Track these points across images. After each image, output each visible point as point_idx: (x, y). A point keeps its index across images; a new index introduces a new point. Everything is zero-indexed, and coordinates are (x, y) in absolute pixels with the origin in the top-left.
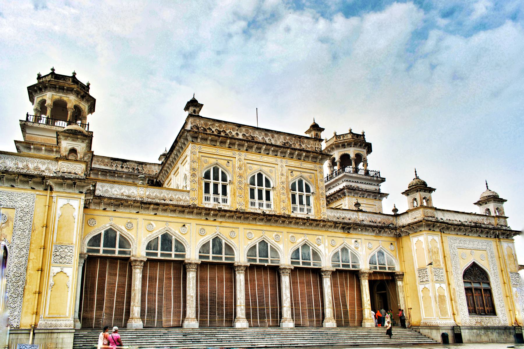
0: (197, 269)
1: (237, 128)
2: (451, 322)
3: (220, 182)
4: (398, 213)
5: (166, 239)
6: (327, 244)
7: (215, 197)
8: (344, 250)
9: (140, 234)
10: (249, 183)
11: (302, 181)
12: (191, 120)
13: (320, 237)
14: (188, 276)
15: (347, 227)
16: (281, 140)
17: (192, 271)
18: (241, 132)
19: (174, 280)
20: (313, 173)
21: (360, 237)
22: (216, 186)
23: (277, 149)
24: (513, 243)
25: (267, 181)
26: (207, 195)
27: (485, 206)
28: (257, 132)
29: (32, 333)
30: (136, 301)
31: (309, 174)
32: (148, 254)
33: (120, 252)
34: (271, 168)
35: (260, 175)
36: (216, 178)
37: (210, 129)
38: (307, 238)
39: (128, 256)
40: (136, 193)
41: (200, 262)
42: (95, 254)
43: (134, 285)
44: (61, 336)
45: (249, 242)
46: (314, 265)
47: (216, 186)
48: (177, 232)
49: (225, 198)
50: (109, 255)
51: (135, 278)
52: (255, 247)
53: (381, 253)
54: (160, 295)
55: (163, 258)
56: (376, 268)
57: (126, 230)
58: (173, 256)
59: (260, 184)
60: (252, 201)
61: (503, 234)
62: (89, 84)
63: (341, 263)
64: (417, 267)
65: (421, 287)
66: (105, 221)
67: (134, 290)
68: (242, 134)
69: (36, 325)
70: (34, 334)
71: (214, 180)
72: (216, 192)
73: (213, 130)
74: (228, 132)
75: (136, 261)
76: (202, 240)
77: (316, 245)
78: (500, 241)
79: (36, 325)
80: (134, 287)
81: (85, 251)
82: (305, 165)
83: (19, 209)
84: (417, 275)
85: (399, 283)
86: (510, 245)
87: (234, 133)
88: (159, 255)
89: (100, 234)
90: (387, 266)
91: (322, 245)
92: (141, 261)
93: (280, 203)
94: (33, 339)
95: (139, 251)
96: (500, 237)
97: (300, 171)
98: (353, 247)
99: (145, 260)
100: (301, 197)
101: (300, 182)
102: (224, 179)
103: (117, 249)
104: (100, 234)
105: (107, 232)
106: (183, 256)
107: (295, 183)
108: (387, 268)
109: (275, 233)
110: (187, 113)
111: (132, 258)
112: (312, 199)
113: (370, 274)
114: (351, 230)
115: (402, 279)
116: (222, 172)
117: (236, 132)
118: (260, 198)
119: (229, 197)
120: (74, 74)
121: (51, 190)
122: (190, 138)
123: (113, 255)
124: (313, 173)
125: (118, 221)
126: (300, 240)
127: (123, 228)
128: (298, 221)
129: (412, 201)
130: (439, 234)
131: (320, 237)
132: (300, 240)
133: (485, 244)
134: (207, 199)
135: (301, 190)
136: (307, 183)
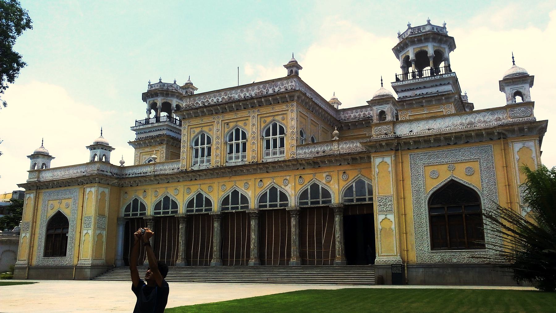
8: (315, 187)
13: (288, 178)
15: (316, 163)
25: (244, 134)
31: (281, 116)
46: (280, 207)
63: (309, 201)
73: (200, 103)
76: (188, 197)
77: (283, 186)
81: (123, 215)
91: (289, 185)
92: (150, 219)
93: (254, 152)
97: (272, 116)
100: (275, 141)
108: (367, 199)
116: (208, 137)
119: (211, 157)
126: (268, 183)
131: (288, 178)
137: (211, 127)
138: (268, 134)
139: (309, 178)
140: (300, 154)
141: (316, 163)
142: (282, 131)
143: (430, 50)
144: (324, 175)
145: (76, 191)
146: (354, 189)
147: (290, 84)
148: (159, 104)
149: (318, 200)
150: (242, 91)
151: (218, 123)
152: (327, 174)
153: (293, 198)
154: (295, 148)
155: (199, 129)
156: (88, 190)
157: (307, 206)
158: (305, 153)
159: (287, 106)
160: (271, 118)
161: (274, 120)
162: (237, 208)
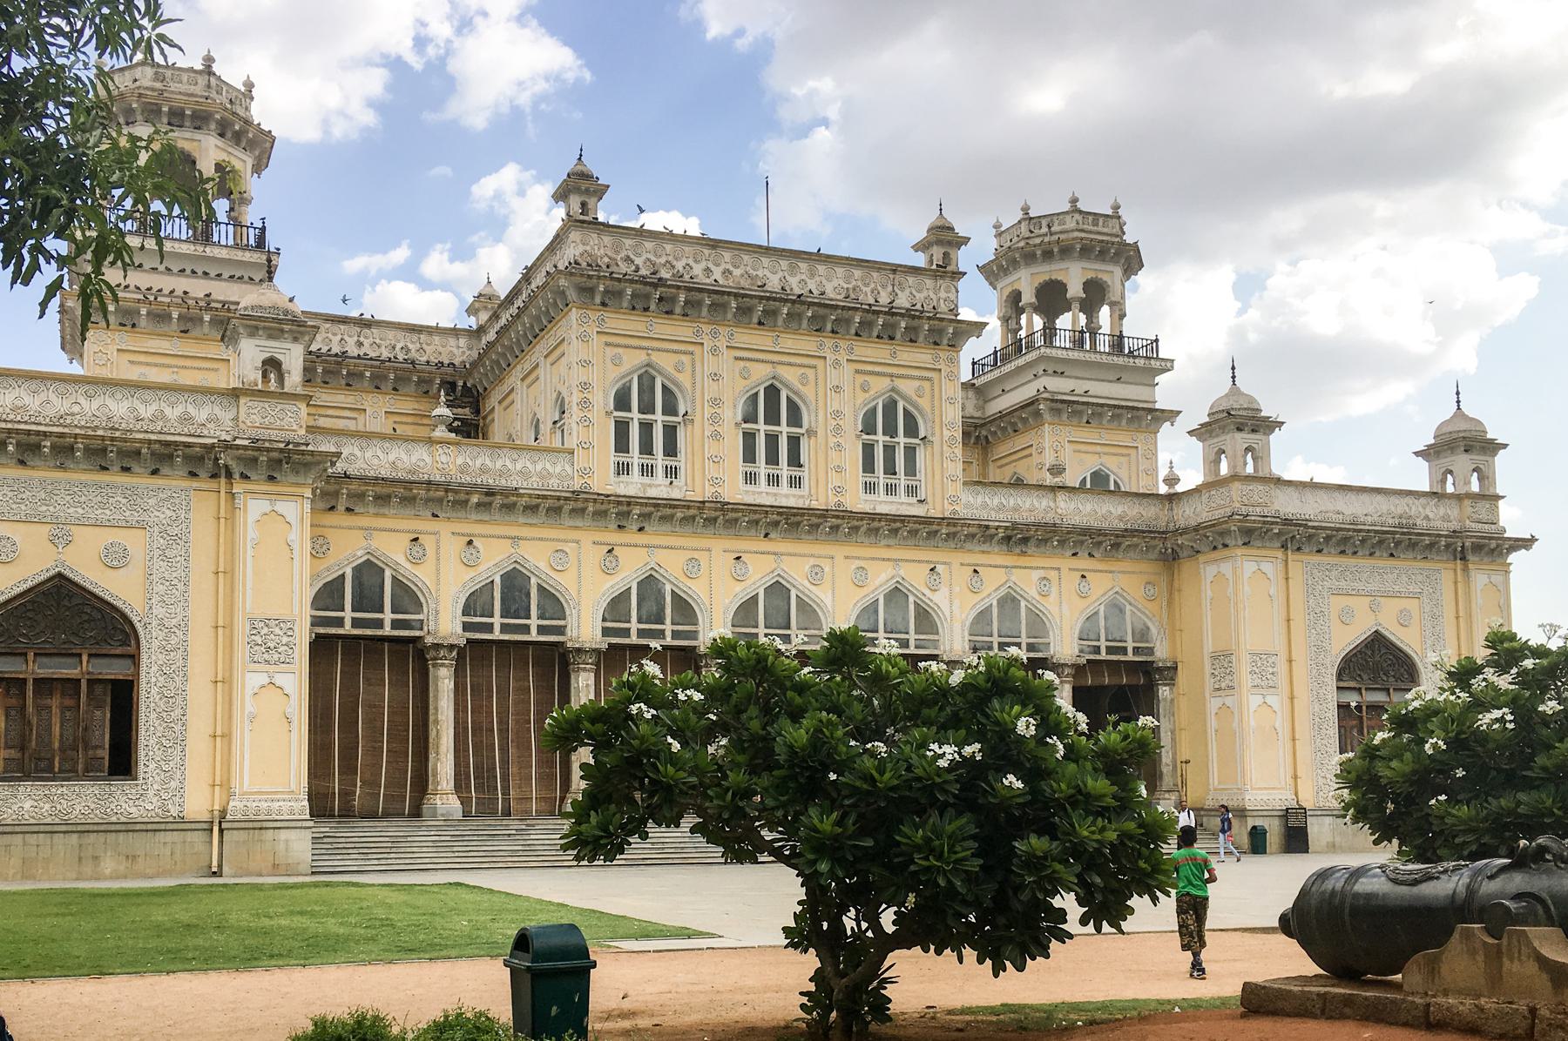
0: (598, 664)
1: (707, 252)
2: (1281, 798)
3: (659, 418)
4: (1179, 488)
5: (515, 584)
6: (957, 589)
7: (645, 462)
8: (1009, 602)
9: (446, 573)
10: (739, 418)
11: (895, 403)
12: (575, 235)
14: (573, 684)
15: (1018, 538)
16: (835, 283)
17: (585, 670)
18: (718, 265)
19: (537, 692)
20: (928, 379)
21: (1055, 562)
22: (646, 428)
23: (822, 311)
24: (1507, 572)
26: (623, 458)
27: (1445, 462)
28: (765, 261)
29: (216, 829)
30: (443, 749)
31: (917, 383)
32: (467, 627)
33: (396, 624)
34: (803, 370)
35: (772, 392)
36: (647, 407)
37: (628, 259)
38: (902, 573)
39: (417, 633)
40: (428, 460)
41: (604, 646)
42: (333, 631)
43: (436, 709)
44: (283, 835)
45: (738, 587)
47: (646, 428)
48: (542, 565)
49: (670, 462)
50: (369, 632)
51: (437, 690)
52: (755, 598)
53: (1116, 608)
54: (504, 731)
55: (506, 637)
56: (1097, 650)
57: (408, 566)
58: (534, 631)
59: (772, 417)
60: (750, 468)
61: (1478, 548)
62: (249, 85)
64: (1209, 647)
65: (1214, 704)
66: (351, 543)
67: (437, 722)
68: (721, 269)
69: (223, 813)
70: (221, 831)
71: (640, 411)
72: (646, 448)
73: (639, 261)
74: (679, 265)
75: (437, 646)
76: (610, 586)
77: (927, 592)
78: (1466, 569)
79: (223, 813)
80: (436, 713)
82: (905, 356)
83: (156, 529)
84: (1208, 669)
85: (1164, 692)
86: (1497, 578)
87: (698, 270)
88: (497, 628)
89: (343, 575)
90: (1130, 645)
91: (944, 590)
92: (452, 647)
94: (221, 842)
95: (445, 622)
96: (1470, 557)
97: (891, 376)
98: (1033, 592)
99: (462, 642)
100: (889, 450)
101: (890, 407)
102: (670, 409)
103: (388, 616)
104: (343, 575)
105: (358, 570)
106: (560, 630)
107: (874, 409)
108: (1130, 651)
109: (812, 561)
110: (560, 212)
111: (429, 640)
112: (920, 455)
113: (1079, 670)
114: (1032, 543)
115: (1171, 682)
117: (703, 265)
118: (772, 459)
119: (682, 461)
121: (229, 475)
122: (572, 295)
123: (379, 632)
124: (928, 379)
125: (386, 540)
127: (401, 560)
128: (876, 524)
129: (1212, 457)
130: (1280, 554)
132: (883, 577)
133: (1420, 578)
134: (623, 469)
135: (890, 430)
136: (910, 408)
137: (684, 358)
138: (869, 428)
139: (1001, 574)
140: (968, 506)
141: (1018, 538)
142: (912, 430)
144: (1036, 575)
145: (190, 504)
146: (1102, 623)
147: (943, 295)
149: (753, 631)
150: (793, 270)
151: (715, 351)
152: (1042, 573)
153: (957, 627)
154: (959, 484)
155: (639, 358)
157: (1123, 658)
158: (985, 506)
159: (936, 359)
160: (885, 383)
161: (893, 390)
162: (626, 633)
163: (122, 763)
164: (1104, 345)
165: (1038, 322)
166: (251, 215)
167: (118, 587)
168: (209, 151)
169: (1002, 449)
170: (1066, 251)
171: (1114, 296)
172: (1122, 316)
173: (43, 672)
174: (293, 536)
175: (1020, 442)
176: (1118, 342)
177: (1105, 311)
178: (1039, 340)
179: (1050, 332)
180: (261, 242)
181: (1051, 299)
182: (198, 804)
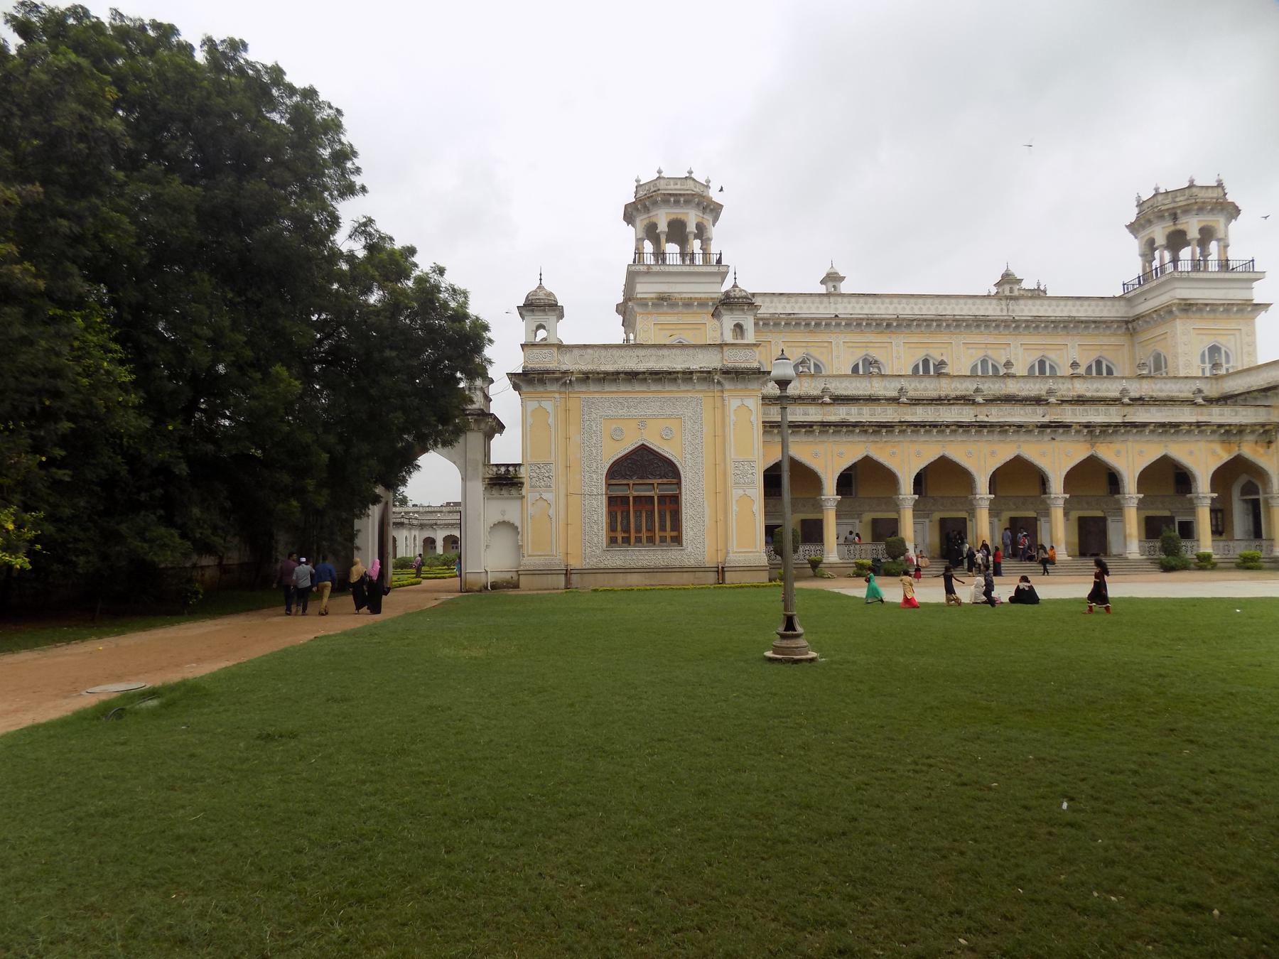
120: (691, 172)
143: (1192, 225)
148: (663, 227)
156: (734, 403)
163: (677, 540)
164: (1213, 266)
165: (1167, 256)
166: (714, 248)
167: (667, 449)
168: (692, 218)
169: (1144, 337)
170: (1186, 210)
171: (1221, 235)
172: (1226, 246)
173: (636, 494)
174: (753, 418)
175: (1159, 331)
176: (1224, 265)
177: (1213, 246)
178: (1170, 268)
179: (1175, 260)
180: (719, 261)
181: (1177, 240)
182: (709, 559)
